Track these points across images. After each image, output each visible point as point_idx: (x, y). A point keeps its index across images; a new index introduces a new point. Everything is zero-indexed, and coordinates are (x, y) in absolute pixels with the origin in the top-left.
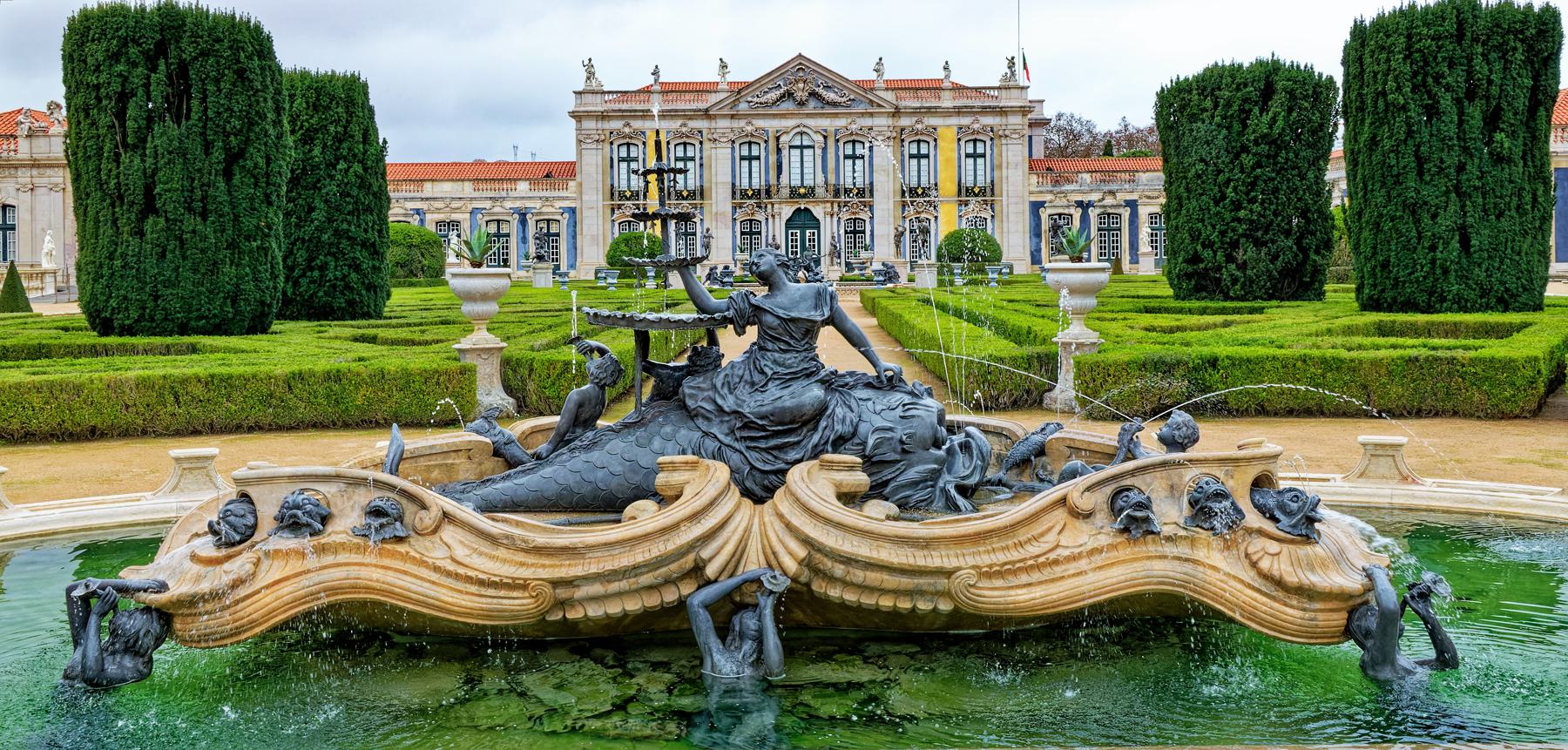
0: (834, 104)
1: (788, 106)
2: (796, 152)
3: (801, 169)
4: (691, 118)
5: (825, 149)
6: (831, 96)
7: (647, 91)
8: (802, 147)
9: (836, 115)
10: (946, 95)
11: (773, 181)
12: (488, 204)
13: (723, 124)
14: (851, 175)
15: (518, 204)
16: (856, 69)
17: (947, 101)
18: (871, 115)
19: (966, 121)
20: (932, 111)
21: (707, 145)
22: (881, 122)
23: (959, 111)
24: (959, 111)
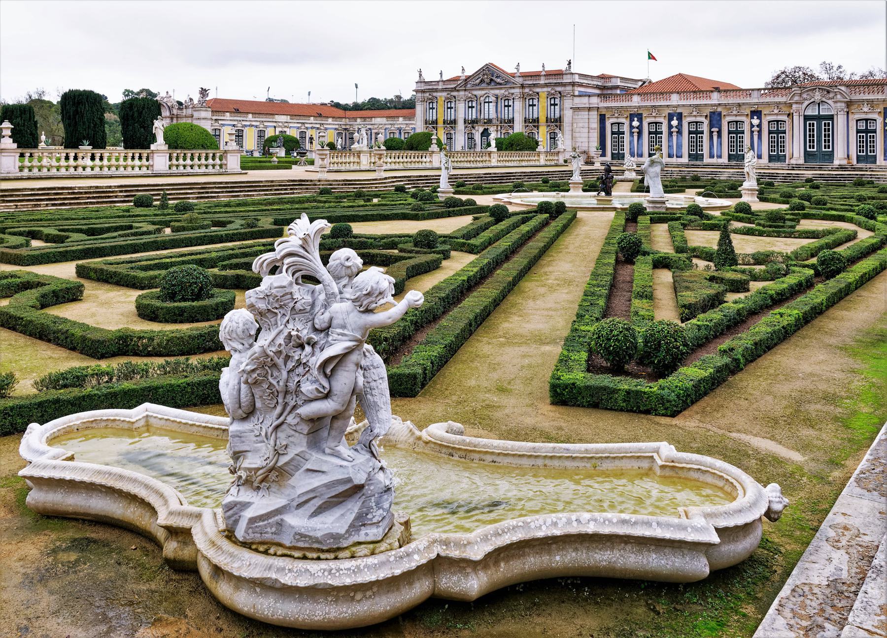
0: (500, 84)
1: (484, 85)
2: (486, 105)
3: (490, 111)
4: (452, 91)
5: (497, 103)
6: (498, 80)
7: (438, 82)
8: (489, 102)
9: (501, 88)
10: (542, 78)
11: (479, 117)
12: (390, 126)
13: (462, 93)
14: (505, 114)
15: (399, 126)
16: (510, 69)
17: (542, 81)
18: (514, 88)
19: (549, 89)
20: (535, 85)
21: (457, 102)
22: (517, 91)
23: (546, 85)
24: (546, 85)
